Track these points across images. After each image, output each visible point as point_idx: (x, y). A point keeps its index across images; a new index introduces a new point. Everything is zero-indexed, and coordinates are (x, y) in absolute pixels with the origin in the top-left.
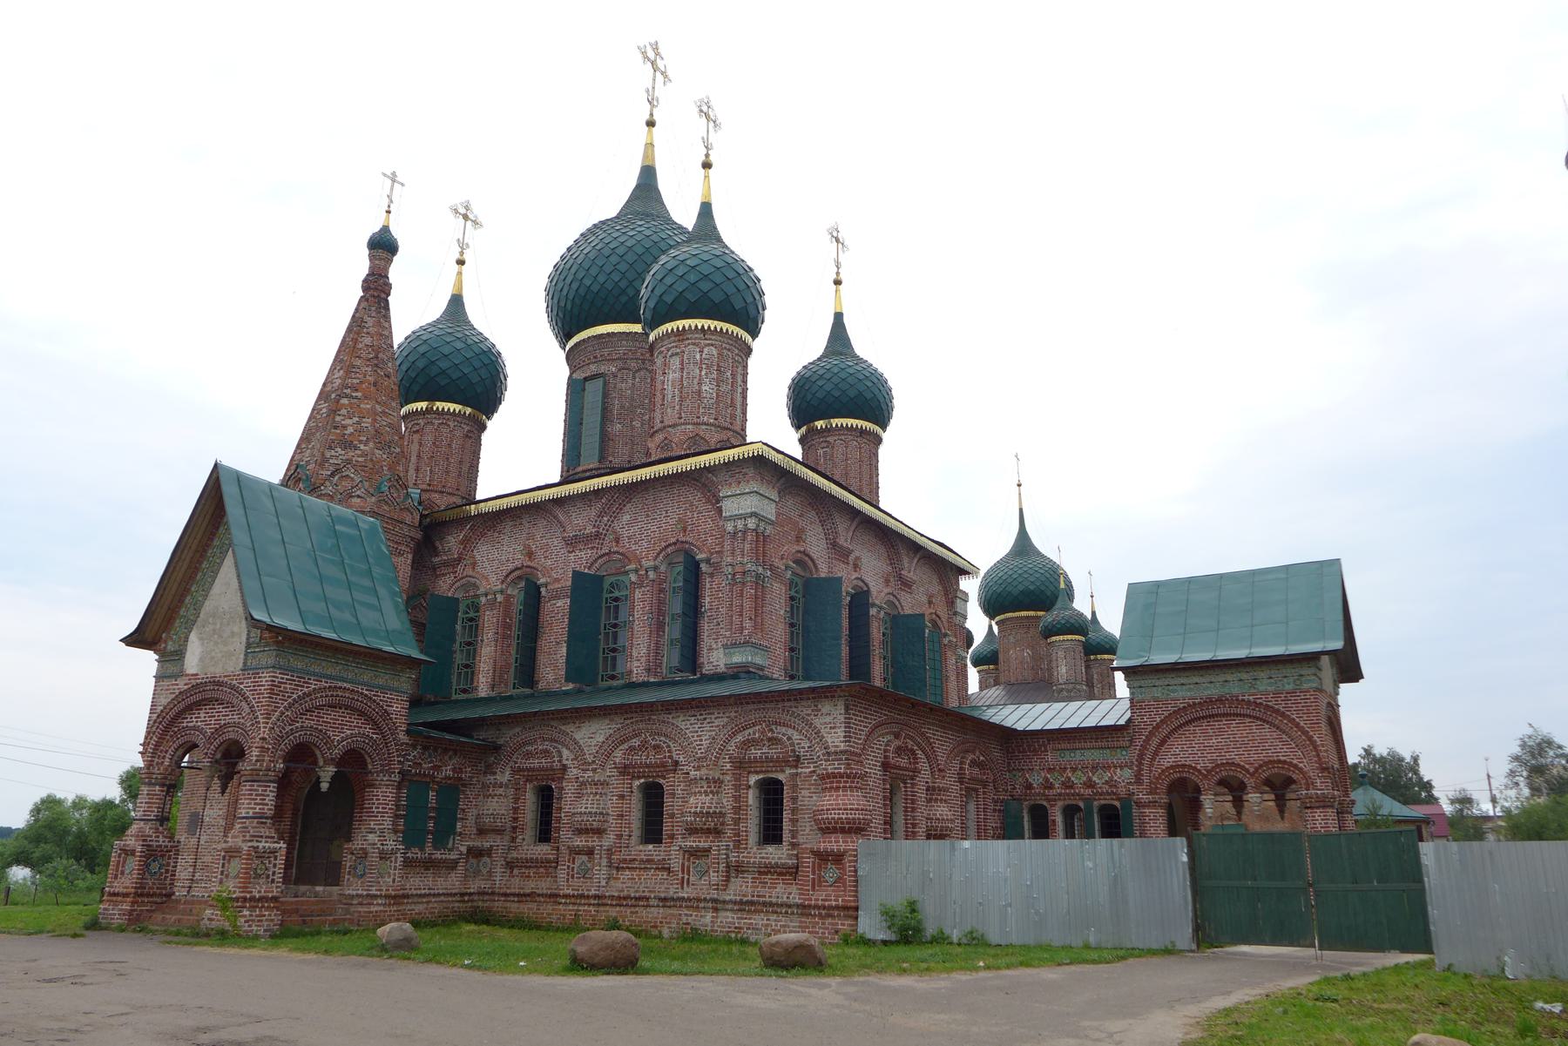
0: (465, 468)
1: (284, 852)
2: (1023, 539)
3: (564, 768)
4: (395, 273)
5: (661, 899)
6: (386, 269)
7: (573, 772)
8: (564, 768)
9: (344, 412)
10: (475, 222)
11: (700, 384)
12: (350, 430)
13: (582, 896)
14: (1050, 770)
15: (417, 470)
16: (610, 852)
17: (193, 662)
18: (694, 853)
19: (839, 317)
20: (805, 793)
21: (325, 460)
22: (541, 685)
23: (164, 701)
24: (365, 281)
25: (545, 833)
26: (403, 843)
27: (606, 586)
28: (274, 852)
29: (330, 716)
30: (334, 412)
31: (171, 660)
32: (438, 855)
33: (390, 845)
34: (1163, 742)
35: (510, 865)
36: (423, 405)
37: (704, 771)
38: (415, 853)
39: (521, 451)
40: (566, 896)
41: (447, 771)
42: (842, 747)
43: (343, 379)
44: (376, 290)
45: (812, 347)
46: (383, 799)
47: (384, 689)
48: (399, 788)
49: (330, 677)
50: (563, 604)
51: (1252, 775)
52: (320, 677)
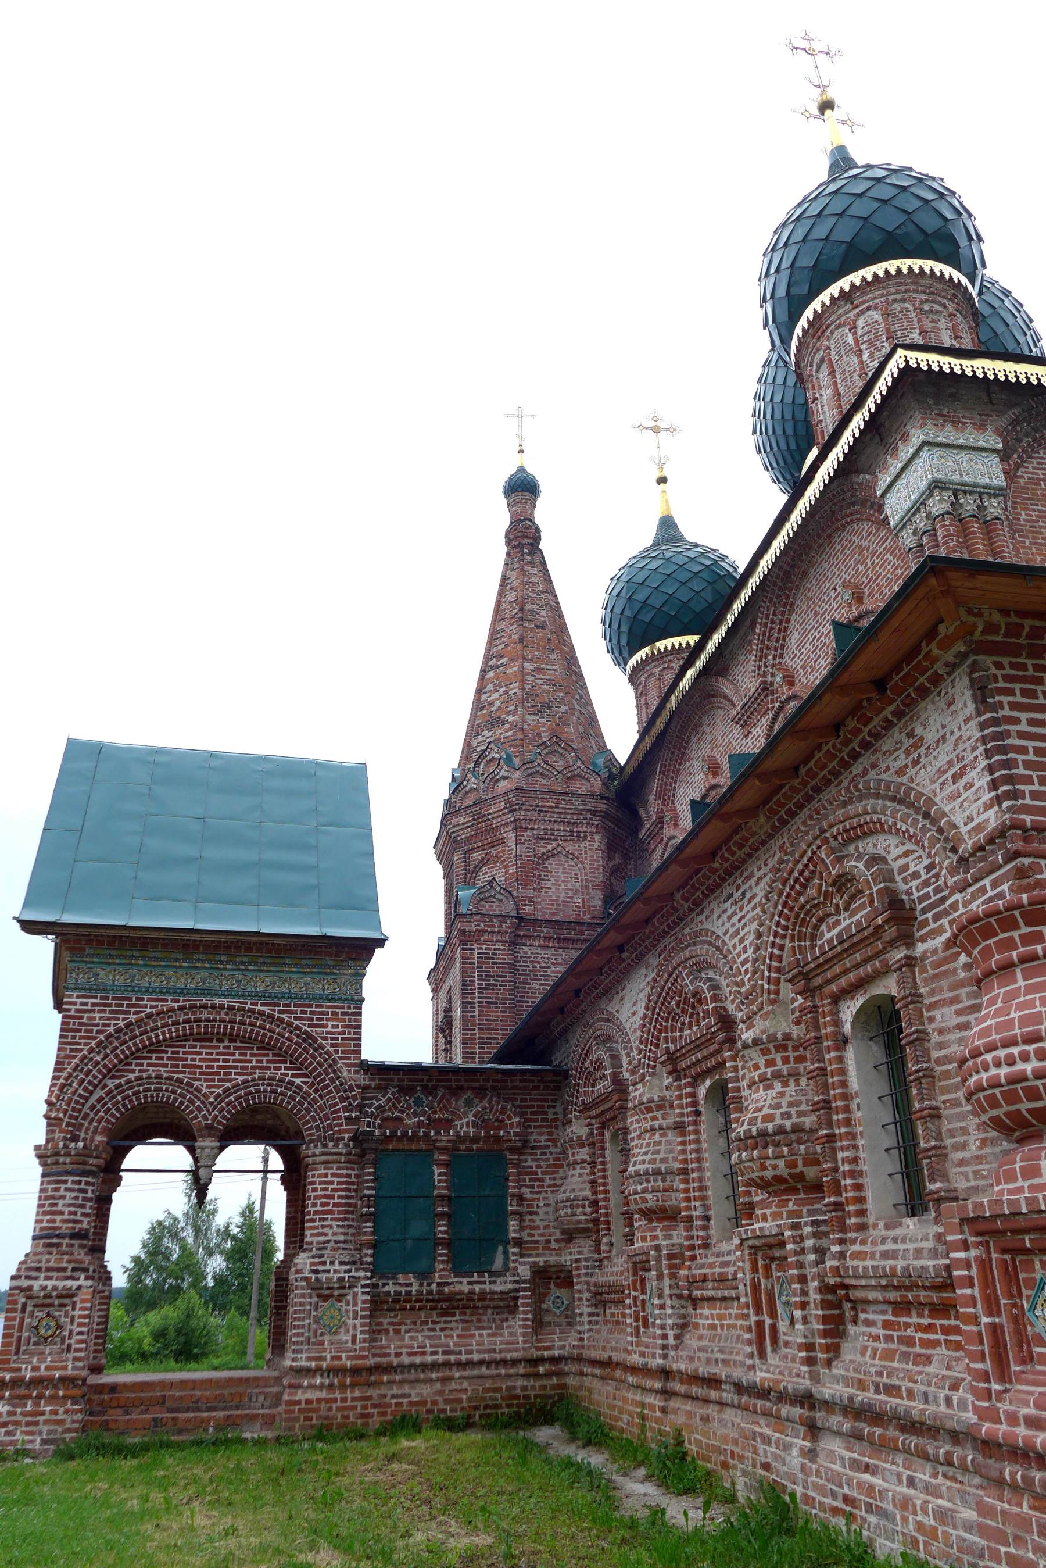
1: (85, 1294)
3: (621, 1087)
6: (532, 514)
9: (490, 687)
10: (671, 430)
20: (945, 1016)
24: (508, 533)
28: (70, 1294)
29: (197, 1056)
32: (463, 1286)
33: (335, 1271)
40: (634, 1370)
41: (465, 1125)
42: (992, 819)
44: (523, 540)
47: (304, 999)
49: (182, 992)
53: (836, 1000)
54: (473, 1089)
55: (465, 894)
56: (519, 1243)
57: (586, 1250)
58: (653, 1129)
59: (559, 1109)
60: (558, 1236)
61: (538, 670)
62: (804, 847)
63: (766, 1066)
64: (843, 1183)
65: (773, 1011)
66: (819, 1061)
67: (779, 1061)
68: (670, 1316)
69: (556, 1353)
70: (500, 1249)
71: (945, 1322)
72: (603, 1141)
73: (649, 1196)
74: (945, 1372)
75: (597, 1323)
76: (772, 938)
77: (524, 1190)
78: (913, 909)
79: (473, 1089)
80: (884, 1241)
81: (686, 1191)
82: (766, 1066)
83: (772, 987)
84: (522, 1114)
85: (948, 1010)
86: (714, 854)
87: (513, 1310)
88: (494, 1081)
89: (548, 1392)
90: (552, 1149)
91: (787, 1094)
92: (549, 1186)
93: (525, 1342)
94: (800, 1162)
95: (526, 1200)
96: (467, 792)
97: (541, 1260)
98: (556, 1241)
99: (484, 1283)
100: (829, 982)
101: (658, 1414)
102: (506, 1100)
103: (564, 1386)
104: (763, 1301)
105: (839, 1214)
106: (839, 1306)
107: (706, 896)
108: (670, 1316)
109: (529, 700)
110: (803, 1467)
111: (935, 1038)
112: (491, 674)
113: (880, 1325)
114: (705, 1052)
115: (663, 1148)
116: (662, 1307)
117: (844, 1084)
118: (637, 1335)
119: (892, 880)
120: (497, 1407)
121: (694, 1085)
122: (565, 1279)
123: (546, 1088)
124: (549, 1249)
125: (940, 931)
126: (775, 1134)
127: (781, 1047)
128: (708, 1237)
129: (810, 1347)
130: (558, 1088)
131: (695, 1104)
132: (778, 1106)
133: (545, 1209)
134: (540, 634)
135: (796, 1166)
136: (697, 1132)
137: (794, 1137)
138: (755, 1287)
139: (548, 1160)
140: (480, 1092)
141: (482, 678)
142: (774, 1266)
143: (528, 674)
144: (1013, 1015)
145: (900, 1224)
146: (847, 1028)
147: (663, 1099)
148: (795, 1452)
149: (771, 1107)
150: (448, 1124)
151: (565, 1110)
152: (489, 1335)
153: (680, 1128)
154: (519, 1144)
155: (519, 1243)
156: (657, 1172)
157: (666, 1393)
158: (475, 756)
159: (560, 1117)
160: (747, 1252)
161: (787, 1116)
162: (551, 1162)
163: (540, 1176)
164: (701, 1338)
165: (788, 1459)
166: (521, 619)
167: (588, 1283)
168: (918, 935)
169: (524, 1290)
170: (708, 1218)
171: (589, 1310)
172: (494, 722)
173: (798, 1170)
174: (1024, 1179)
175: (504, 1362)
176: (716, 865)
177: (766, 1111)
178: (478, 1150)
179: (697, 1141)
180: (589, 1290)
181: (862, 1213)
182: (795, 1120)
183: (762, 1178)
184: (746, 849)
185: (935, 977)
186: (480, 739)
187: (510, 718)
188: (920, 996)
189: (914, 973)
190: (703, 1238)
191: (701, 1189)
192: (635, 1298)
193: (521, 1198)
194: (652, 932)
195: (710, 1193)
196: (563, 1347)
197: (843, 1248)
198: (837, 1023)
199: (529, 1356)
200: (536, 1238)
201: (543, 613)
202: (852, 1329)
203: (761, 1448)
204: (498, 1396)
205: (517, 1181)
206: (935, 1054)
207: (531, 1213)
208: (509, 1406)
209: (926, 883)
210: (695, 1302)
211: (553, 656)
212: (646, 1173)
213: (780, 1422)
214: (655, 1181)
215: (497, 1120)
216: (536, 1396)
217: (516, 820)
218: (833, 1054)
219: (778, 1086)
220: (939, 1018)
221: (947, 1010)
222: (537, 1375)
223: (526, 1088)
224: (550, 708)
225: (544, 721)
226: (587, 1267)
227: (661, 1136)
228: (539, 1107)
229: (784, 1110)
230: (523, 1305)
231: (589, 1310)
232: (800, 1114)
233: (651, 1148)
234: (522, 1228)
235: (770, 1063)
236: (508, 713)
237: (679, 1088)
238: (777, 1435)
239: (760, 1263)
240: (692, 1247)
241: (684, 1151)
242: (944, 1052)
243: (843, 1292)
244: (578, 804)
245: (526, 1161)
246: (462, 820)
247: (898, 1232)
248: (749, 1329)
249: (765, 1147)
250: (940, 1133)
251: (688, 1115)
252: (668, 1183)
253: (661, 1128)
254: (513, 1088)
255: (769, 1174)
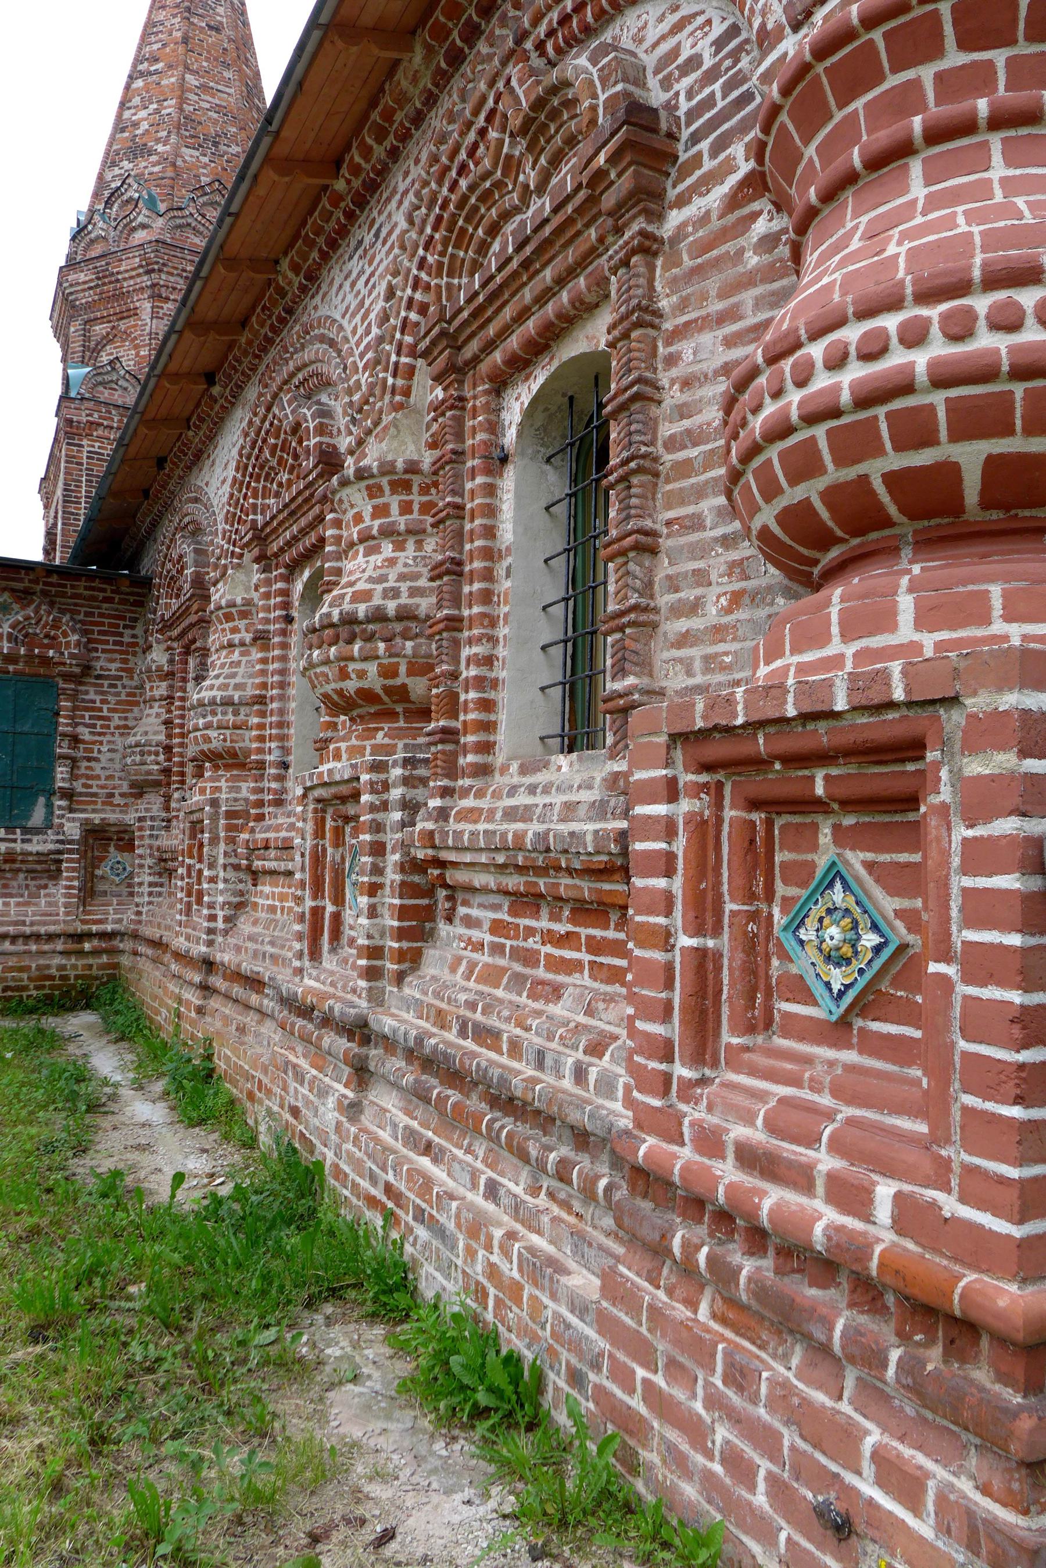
9: (137, 101)
53: (500, 384)
54: (13, 590)
55: (78, 373)
56: (68, 794)
57: (155, 807)
58: (231, 645)
59: (139, 631)
60: (125, 788)
61: (204, 88)
62: (483, 86)
63: (374, 517)
64: (463, 697)
65: (395, 423)
66: (454, 493)
67: (395, 509)
68: (222, 892)
69: (109, 928)
70: (42, 800)
71: (597, 933)
72: (185, 671)
73: (213, 734)
74: (582, 1019)
75: (160, 894)
76: (409, 291)
77: (81, 729)
78: (672, 136)
79: (13, 590)
80: (513, 791)
81: (261, 726)
82: (374, 517)
83: (400, 382)
84: (85, 632)
85: (708, 338)
86: (338, 164)
87: (55, 875)
88: (45, 584)
89: (95, 972)
90: (125, 681)
91: (401, 562)
92: (117, 727)
93: (67, 914)
94: (403, 669)
95: (83, 742)
96: (92, 241)
97: (96, 818)
98: (122, 795)
99: (15, 841)
100: (490, 346)
101: (193, 1014)
102: (63, 612)
103: (116, 966)
104: (326, 879)
105: (449, 747)
106: (430, 893)
107: (325, 257)
108: (222, 892)
109: (187, 125)
110: (338, 1125)
111: (673, 396)
112: (139, 83)
113: (486, 926)
114: (303, 522)
115: (241, 670)
116: (213, 880)
117: (490, 532)
118: (188, 912)
119: (640, 82)
120: (25, 988)
121: (288, 578)
123: (122, 602)
124: (111, 804)
125: (728, 167)
126: (369, 620)
127: (401, 486)
128: (284, 791)
129: (375, 952)
130: (141, 604)
131: (286, 605)
132: (382, 579)
133: (109, 755)
134: (212, 38)
135: (395, 674)
136: (285, 646)
137: (398, 627)
138: (318, 858)
139: (118, 694)
140: (24, 596)
141: (127, 87)
142: (348, 830)
143: (190, 91)
144: (892, 249)
145: (546, 765)
146: (510, 437)
147: (248, 602)
148: (331, 1102)
149: (370, 580)
151: (146, 631)
152: (18, 904)
153: (261, 639)
154: (77, 670)
155: (68, 794)
156: (227, 702)
157: (205, 989)
158: (107, 194)
159: (141, 641)
160: (311, 807)
161: (395, 593)
162: (123, 697)
163: (105, 713)
164: (255, 923)
165: (322, 1109)
166: (188, 10)
167: (151, 847)
168: (672, 194)
169: (70, 851)
170: (285, 766)
171: (151, 879)
172: (138, 150)
173: (398, 681)
174: (847, 637)
175: (37, 937)
176: (340, 185)
177: (361, 586)
178: (15, 673)
179: (284, 659)
180: (151, 855)
181: (486, 748)
182: (404, 600)
183: (340, 692)
184: (391, 140)
185: (697, 271)
186: (117, 171)
187: (160, 148)
188: (658, 314)
189: (652, 269)
190: (276, 792)
191: (280, 725)
192: (189, 868)
193: (75, 740)
194: (250, 343)
195: (292, 731)
196: (120, 921)
197: (448, 802)
198: (494, 427)
199: (70, 930)
200: (94, 790)
201: (220, 10)
202: (443, 929)
203: (293, 1085)
204: (25, 976)
205: (72, 718)
206: (666, 430)
207: (89, 759)
208: (37, 988)
209: (711, 76)
210: (255, 876)
211: (227, 74)
212: (213, 702)
213: (320, 1057)
214: (224, 713)
215: (47, 636)
216: (77, 977)
217: (154, 285)
218: (480, 480)
219: (387, 549)
220: (688, 356)
221: (707, 338)
222: (81, 953)
223: (93, 598)
224: (216, 144)
225: (205, 160)
226: (152, 828)
227: (242, 654)
228: (110, 625)
229: (390, 584)
230: (68, 869)
231: (151, 879)
232: (414, 592)
233: (226, 670)
234: (74, 777)
235: (381, 511)
236: (158, 141)
237: (268, 582)
238: (314, 1072)
239: (329, 824)
240: (260, 804)
241: (263, 672)
242: (686, 423)
243: (436, 872)
245: (87, 693)
246: (82, 277)
247: (541, 778)
248: (301, 918)
249: (350, 641)
250: (650, 584)
251: (276, 620)
252: (242, 717)
253: (242, 644)
254: (75, 596)
255: (351, 686)
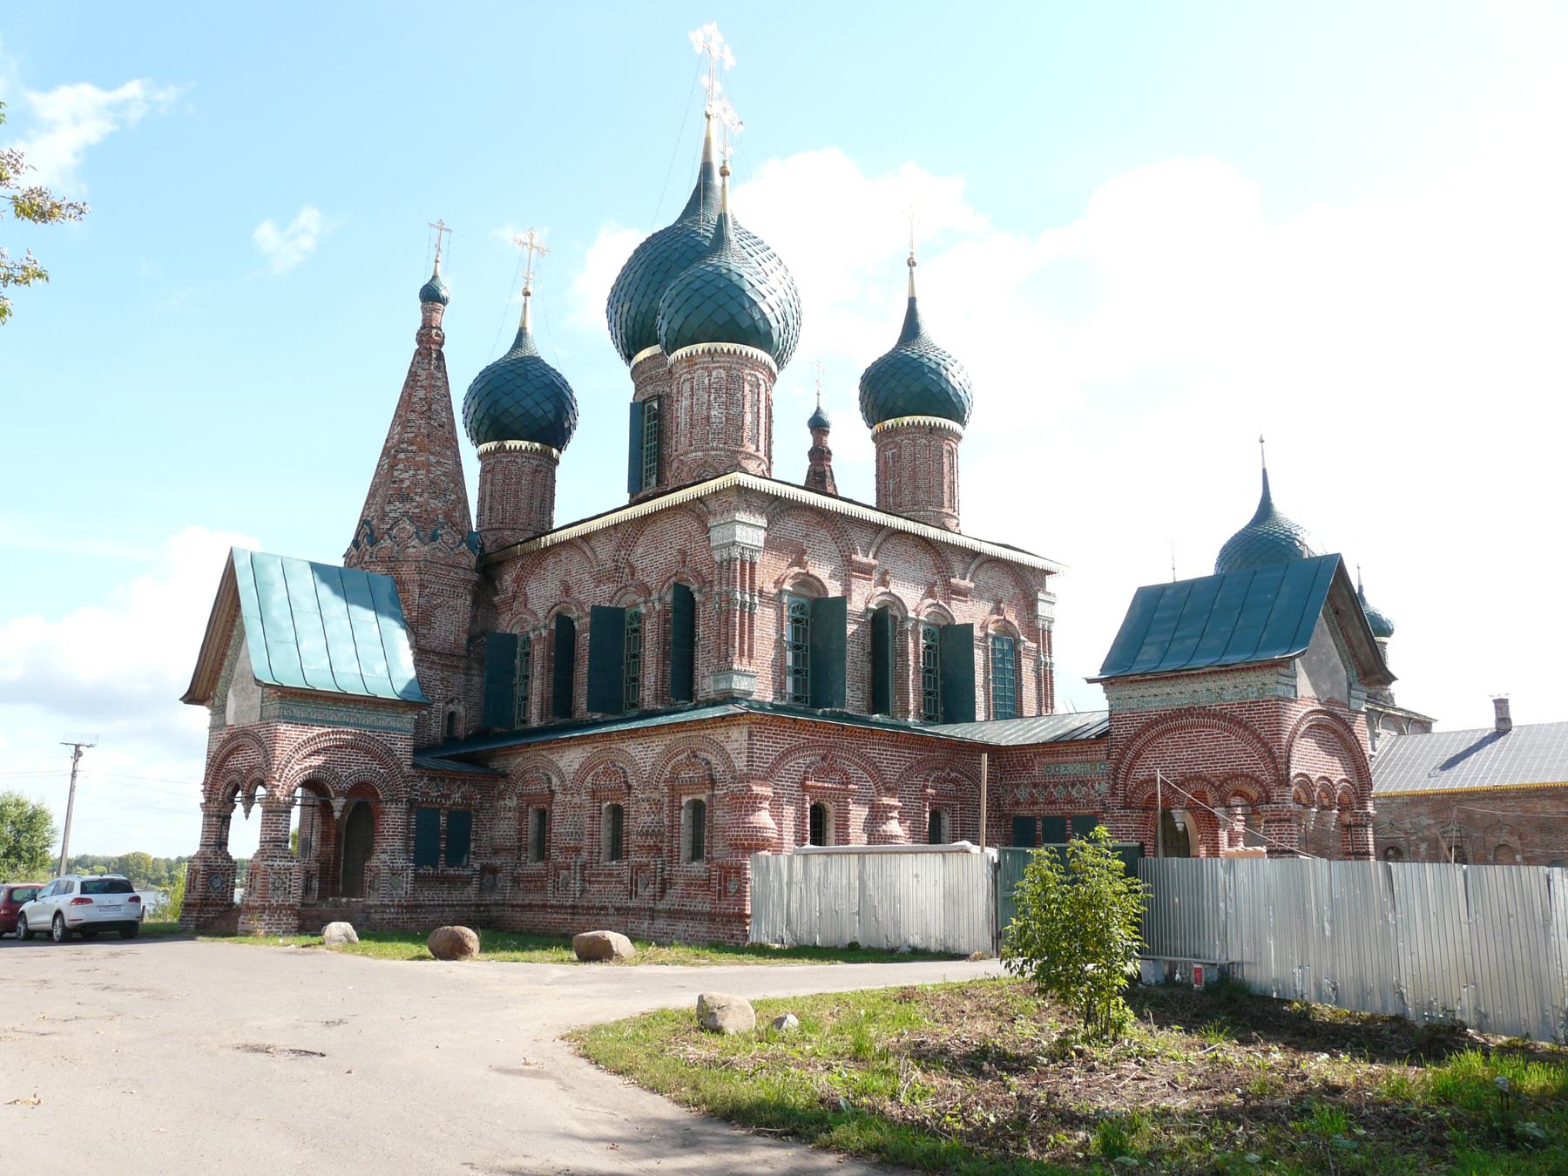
0: (536, 504)
2: (1266, 509)
4: (449, 321)
5: (618, 909)
7: (559, 797)
8: (552, 793)
9: (401, 466)
11: (709, 409)
12: (407, 483)
13: (562, 907)
14: (1035, 785)
15: (491, 509)
16: (584, 867)
17: (230, 718)
18: (640, 868)
19: (912, 302)
21: (385, 514)
22: (577, 715)
23: (215, 748)
25: (542, 852)
26: (414, 861)
27: (627, 619)
30: (392, 467)
31: (219, 711)
32: (451, 871)
34: (1138, 755)
35: (516, 881)
36: (492, 445)
37: (648, 794)
38: (428, 870)
39: (591, 481)
40: (552, 906)
41: (457, 797)
43: (400, 434)
45: (885, 341)
46: (393, 820)
48: (409, 811)
50: (587, 635)
51: (1217, 789)
52: (322, 723)
122: (494, 871)
150: (447, 797)
244: (461, 572)
